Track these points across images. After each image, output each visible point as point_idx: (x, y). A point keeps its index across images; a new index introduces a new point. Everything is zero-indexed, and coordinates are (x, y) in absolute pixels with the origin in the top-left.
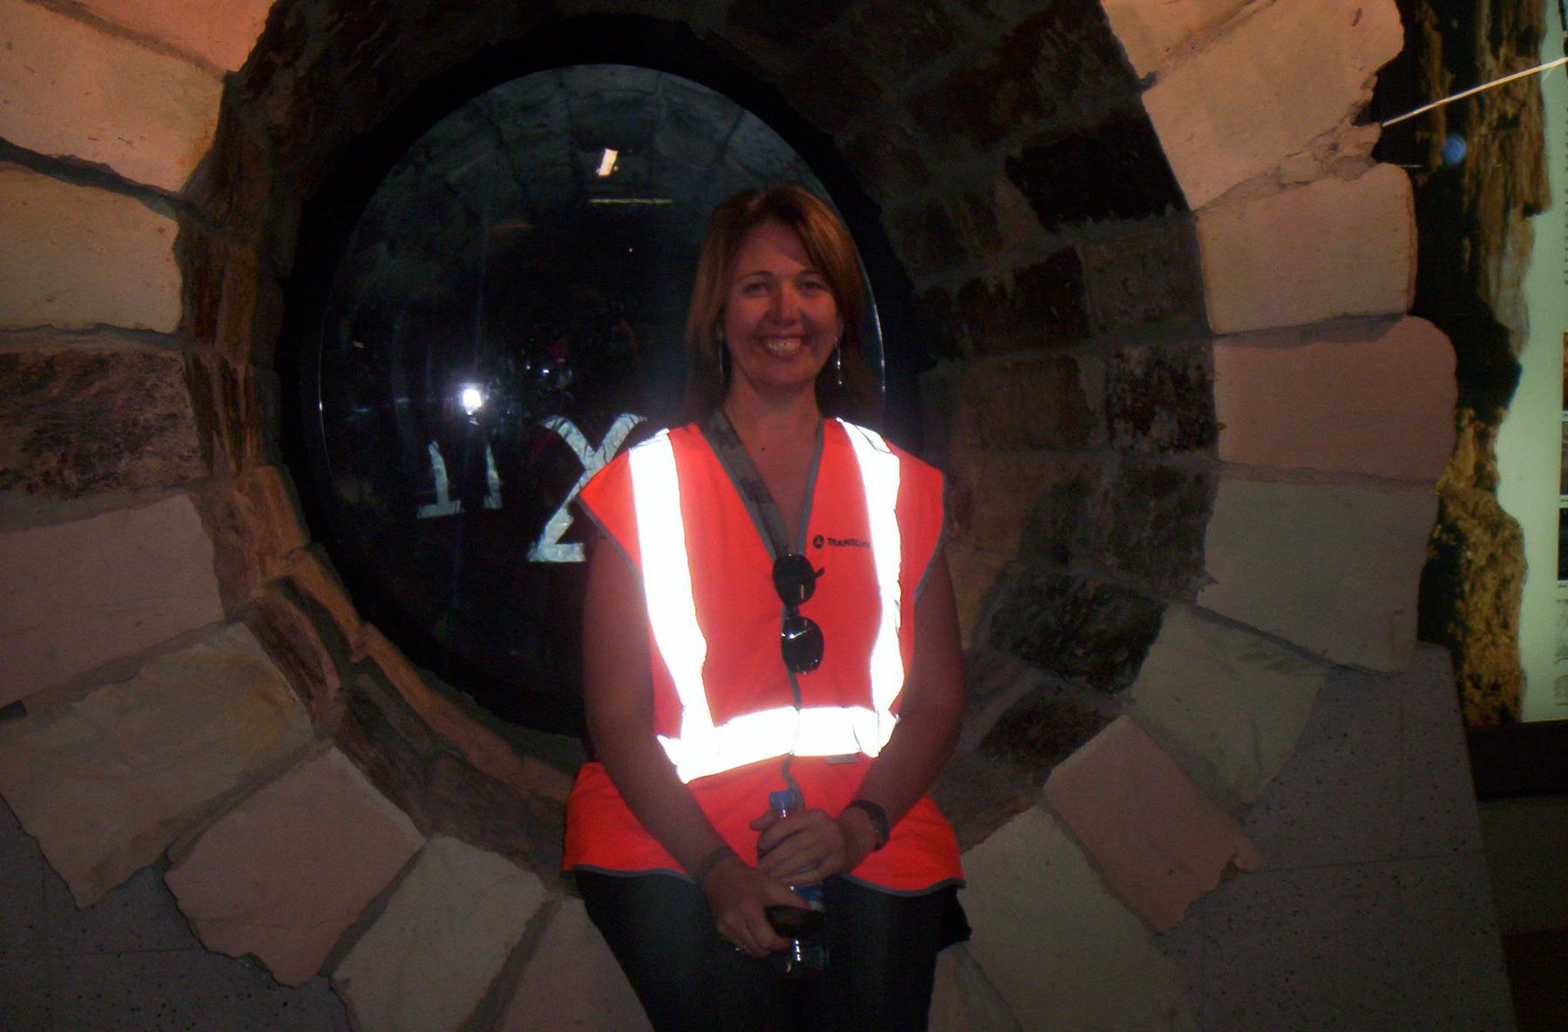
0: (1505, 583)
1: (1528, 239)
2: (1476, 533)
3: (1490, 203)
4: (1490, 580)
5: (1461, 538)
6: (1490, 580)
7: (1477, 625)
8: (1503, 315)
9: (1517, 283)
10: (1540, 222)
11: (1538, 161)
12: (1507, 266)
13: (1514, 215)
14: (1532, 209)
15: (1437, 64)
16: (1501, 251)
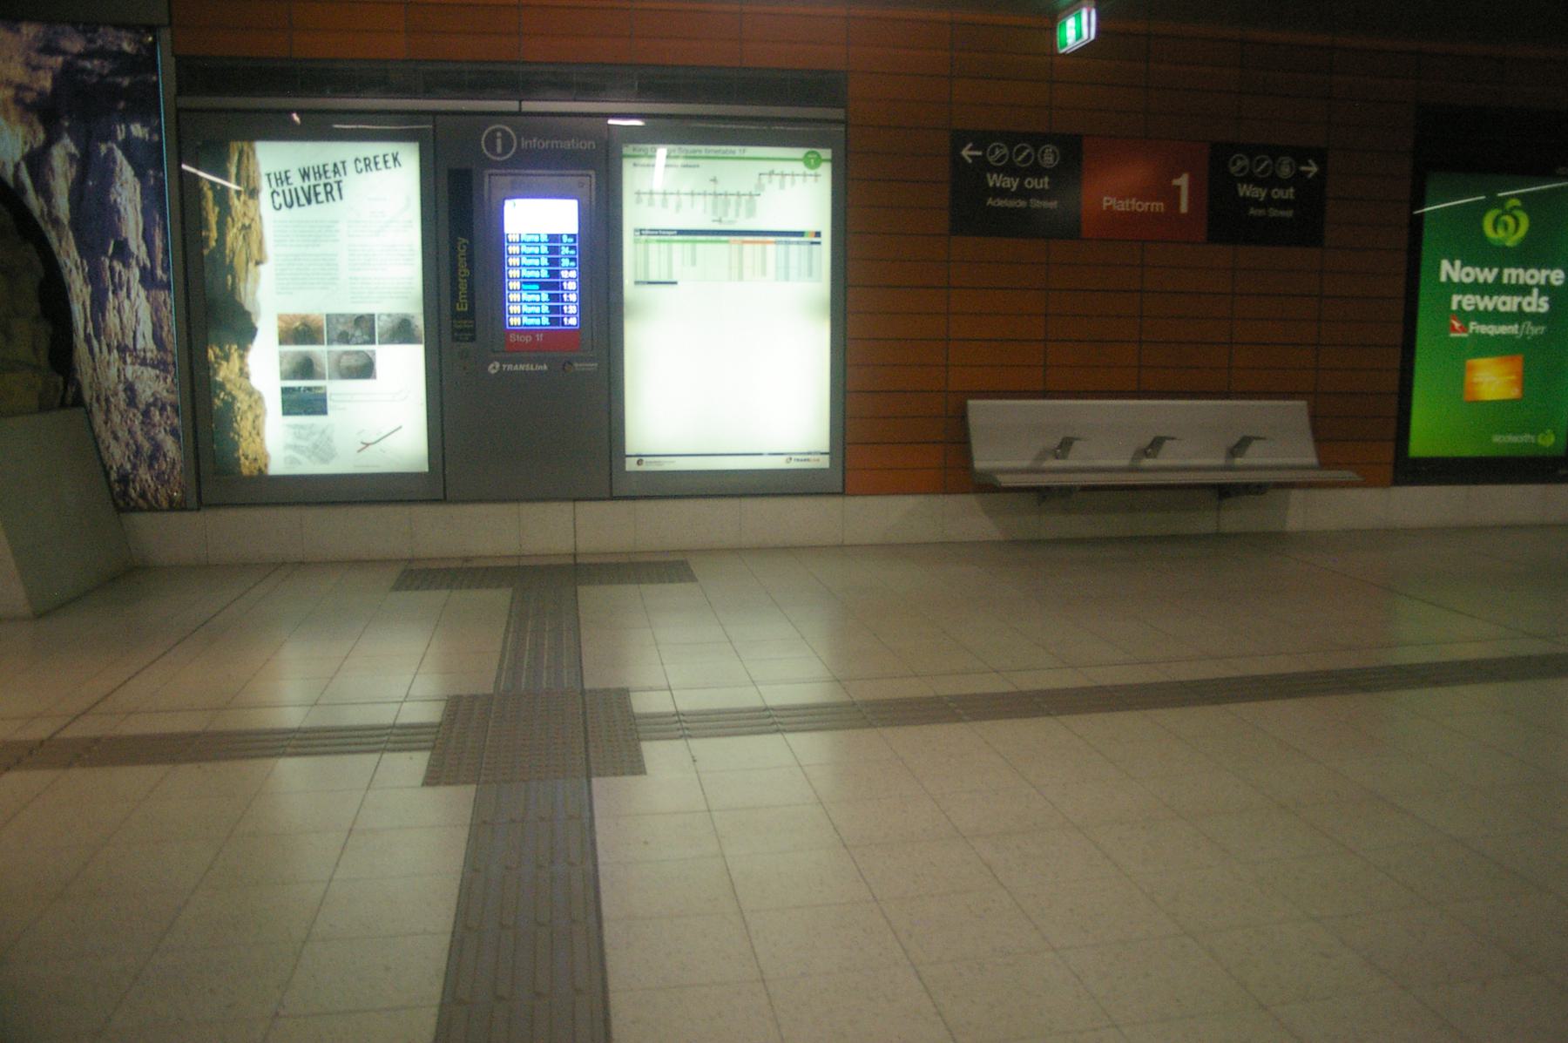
0: (257, 417)
1: (258, 275)
2: (241, 396)
3: (239, 261)
4: (250, 416)
5: (234, 398)
6: (250, 416)
7: (245, 433)
8: (248, 307)
9: (254, 293)
10: (262, 268)
11: (261, 243)
12: (249, 286)
13: (251, 265)
14: (258, 263)
15: (210, 204)
16: (246, 279)
